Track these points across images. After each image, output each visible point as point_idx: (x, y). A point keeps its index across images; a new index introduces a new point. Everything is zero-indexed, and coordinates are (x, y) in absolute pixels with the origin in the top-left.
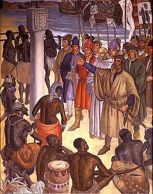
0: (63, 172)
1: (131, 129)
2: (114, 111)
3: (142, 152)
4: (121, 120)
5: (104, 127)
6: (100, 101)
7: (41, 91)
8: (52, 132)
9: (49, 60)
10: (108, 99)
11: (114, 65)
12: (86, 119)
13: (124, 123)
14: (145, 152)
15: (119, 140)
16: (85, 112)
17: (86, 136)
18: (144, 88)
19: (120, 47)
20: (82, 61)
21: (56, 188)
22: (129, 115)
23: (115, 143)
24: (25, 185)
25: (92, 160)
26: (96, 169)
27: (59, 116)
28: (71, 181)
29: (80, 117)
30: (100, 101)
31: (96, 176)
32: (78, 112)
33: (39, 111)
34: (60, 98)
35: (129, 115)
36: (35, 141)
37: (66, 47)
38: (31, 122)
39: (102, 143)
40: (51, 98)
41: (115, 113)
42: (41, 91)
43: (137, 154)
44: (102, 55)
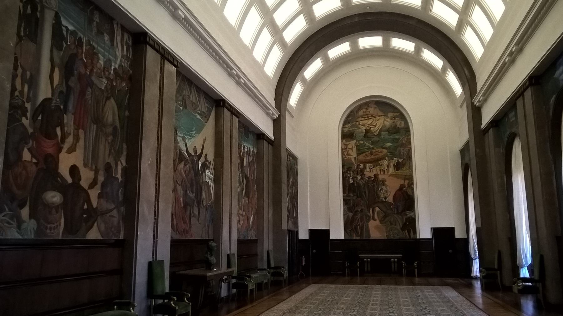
0: (57, 208)
7: (44, 92)
8: (50, 151)
9: (55, 52)
13: (109, 155)
21: (48, 231)
24: (15, 224)
27: (58, 130)
28: (63, 220)
29: (77, 138)
33: (40, 118)
36: (32, 159)
38: (30, 131)
42: (44, 92)
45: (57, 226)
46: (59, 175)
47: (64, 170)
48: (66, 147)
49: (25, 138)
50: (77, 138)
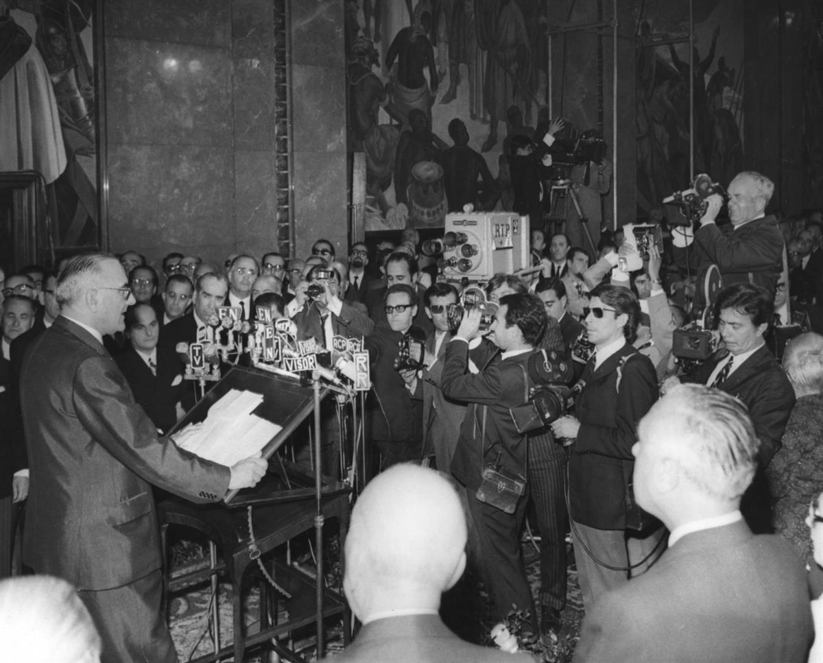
6: (483, 49)
13: (514, 95)
15: (508, 127)
26: (480, 178)
27: (426, 72)
29: (456, 79)
30: (483, 49)
31: (480, 192)
33: (396, 60)
34: (428, 36)
36: (391, 121)
38: (385, 81)
40: (414, 35)
45: (438, 209)
46: (434, 137)
47: (440, 129)
48: (439, 97)
49: (379, 92)
50: (456, 79)
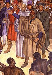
1: (41, 52)
2: (31, 41)
3: (47, 66)
4: (35, 47)
5: (25, 51)
6: (22, 35)
10: (27, 35)
11: (31, 14)
12: (14, 47)
13: (37, 48)
14: (49, 66)
15: (34, 59)
16: (13, 42)
17: (14, 57)
18: (48, 28)
19: (34, 4)
20: (12, 12)
22: (39, 44)
23: (31, 60)
25: (18, 70)
29: (10, 45)
30: (22, 35)
32: (9, 42)
35: (39, 44)
37: (2, 4)
39: (23, 61)
41: (31, 43)
43: (44, 67)
44: (24, 8)
